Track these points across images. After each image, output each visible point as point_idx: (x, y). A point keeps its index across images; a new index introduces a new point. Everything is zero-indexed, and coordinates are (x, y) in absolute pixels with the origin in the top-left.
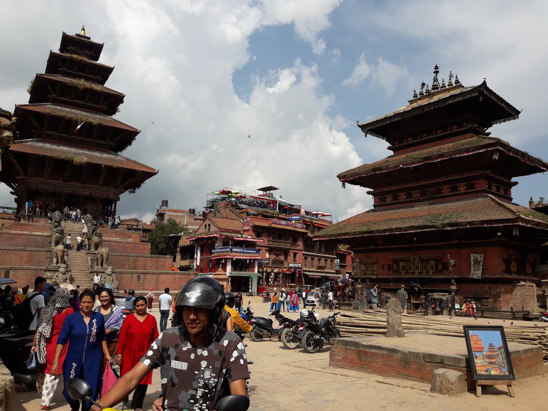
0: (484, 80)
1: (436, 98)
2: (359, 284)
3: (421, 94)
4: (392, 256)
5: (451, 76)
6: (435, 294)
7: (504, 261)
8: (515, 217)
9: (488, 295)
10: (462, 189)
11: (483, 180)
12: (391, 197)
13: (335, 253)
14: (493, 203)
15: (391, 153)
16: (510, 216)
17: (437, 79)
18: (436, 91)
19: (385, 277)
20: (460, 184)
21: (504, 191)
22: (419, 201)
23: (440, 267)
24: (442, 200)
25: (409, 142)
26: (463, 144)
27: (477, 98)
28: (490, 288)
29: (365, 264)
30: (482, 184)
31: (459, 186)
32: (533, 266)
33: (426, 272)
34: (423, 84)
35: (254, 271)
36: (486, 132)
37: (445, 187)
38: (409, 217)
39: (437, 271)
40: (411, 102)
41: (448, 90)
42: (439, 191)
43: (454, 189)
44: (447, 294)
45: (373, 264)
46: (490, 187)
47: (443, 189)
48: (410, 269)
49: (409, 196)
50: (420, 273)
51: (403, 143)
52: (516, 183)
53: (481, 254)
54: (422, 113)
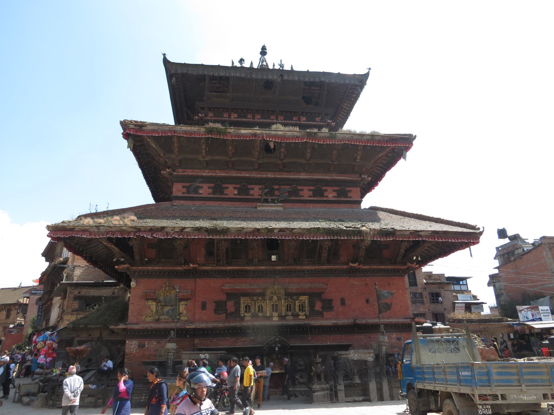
0: (368, 70)
2: (169, 342)
10: (330, 195)
12: (209, 188)
19: (210, 325)
22: (266, 201)
23: (318, 306)
24: (299, 205)
28: (399, 339)
31: (326, 190)
33: (292, 315)
34: (241, 61)
37: (306, 188)
39: (313, 313)
42: (295, 192)
43: (318, 192)
45: (181, 300)
47: (302, 190)
50: (281, 317)
54: (279, 80)
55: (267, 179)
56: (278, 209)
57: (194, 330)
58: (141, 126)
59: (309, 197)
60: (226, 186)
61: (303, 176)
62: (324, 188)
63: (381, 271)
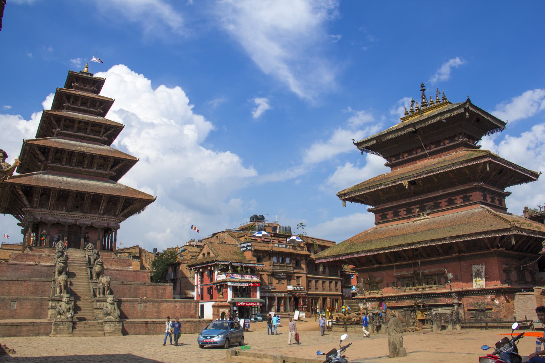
1: (426, 114)
3: (412, 111)
4: (396, 273)
5: (438, 93)
6: (440, 309)
7: (504, 271)
8: (510, 226)
9: (489, 307)
10: (459, 202)
11: (477, 192)
12: (392, 213)
13: (339, 274)
14: (489, 214)
15: (389, 168)
16: (506, 226)
17: (425, 96)
18: (425, 108)
20: (456, 197)
21: (497, 202)
22: (419, 216)
25: (405, 158)
26: (455, 157)
27: (464, 113)
29: (370, 284)
30: (477, 196)
31: (456, 199)
32: (532, 274)
35: (256, 297)
36: (477, 145)
37: (443, 201)
38: (410, 233)
40: (403, 119)
41: (436, 107)
44: (451, 308)
46: (485, 198)
47: (441, 203)
48: (414, 285)
49: (409, 211)
51: (400, 158)
52: (509, 194)
53: (482, 265)
54: (414, 130)
55: (419, 201)
56: (425, 220)
57: (383, 297)
58: (345, 194)
59: (446, 206)
60: (400, 210)
61: (440, 193)
62: (453, 198)
63: (478, 254)
